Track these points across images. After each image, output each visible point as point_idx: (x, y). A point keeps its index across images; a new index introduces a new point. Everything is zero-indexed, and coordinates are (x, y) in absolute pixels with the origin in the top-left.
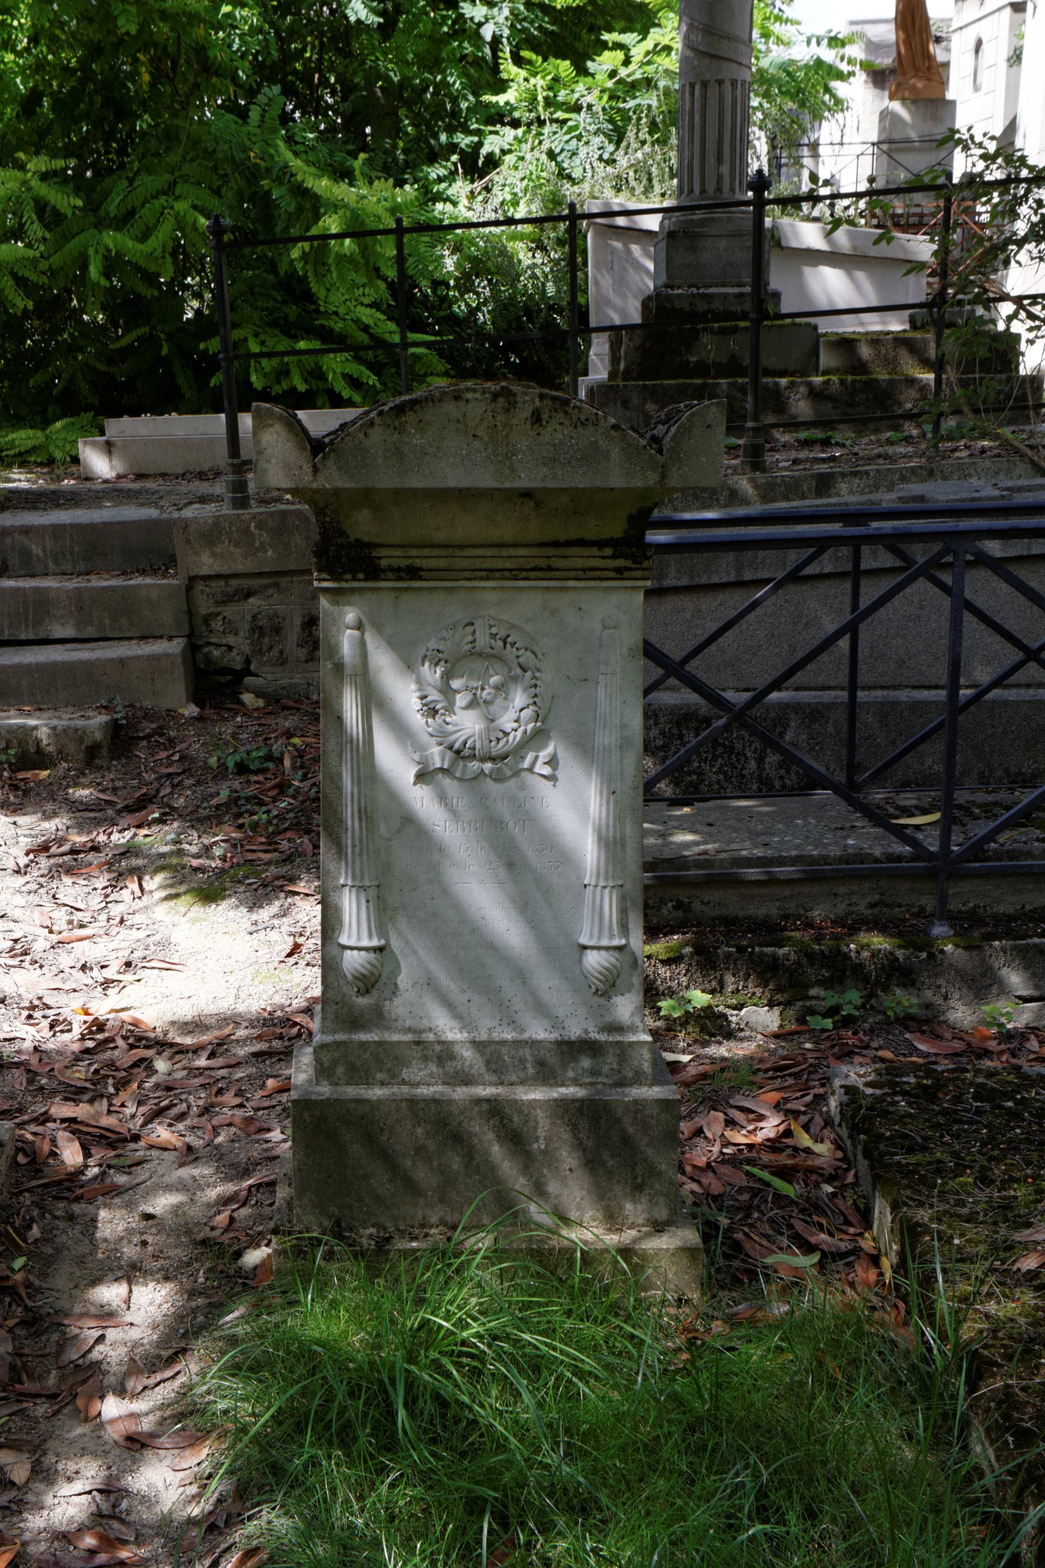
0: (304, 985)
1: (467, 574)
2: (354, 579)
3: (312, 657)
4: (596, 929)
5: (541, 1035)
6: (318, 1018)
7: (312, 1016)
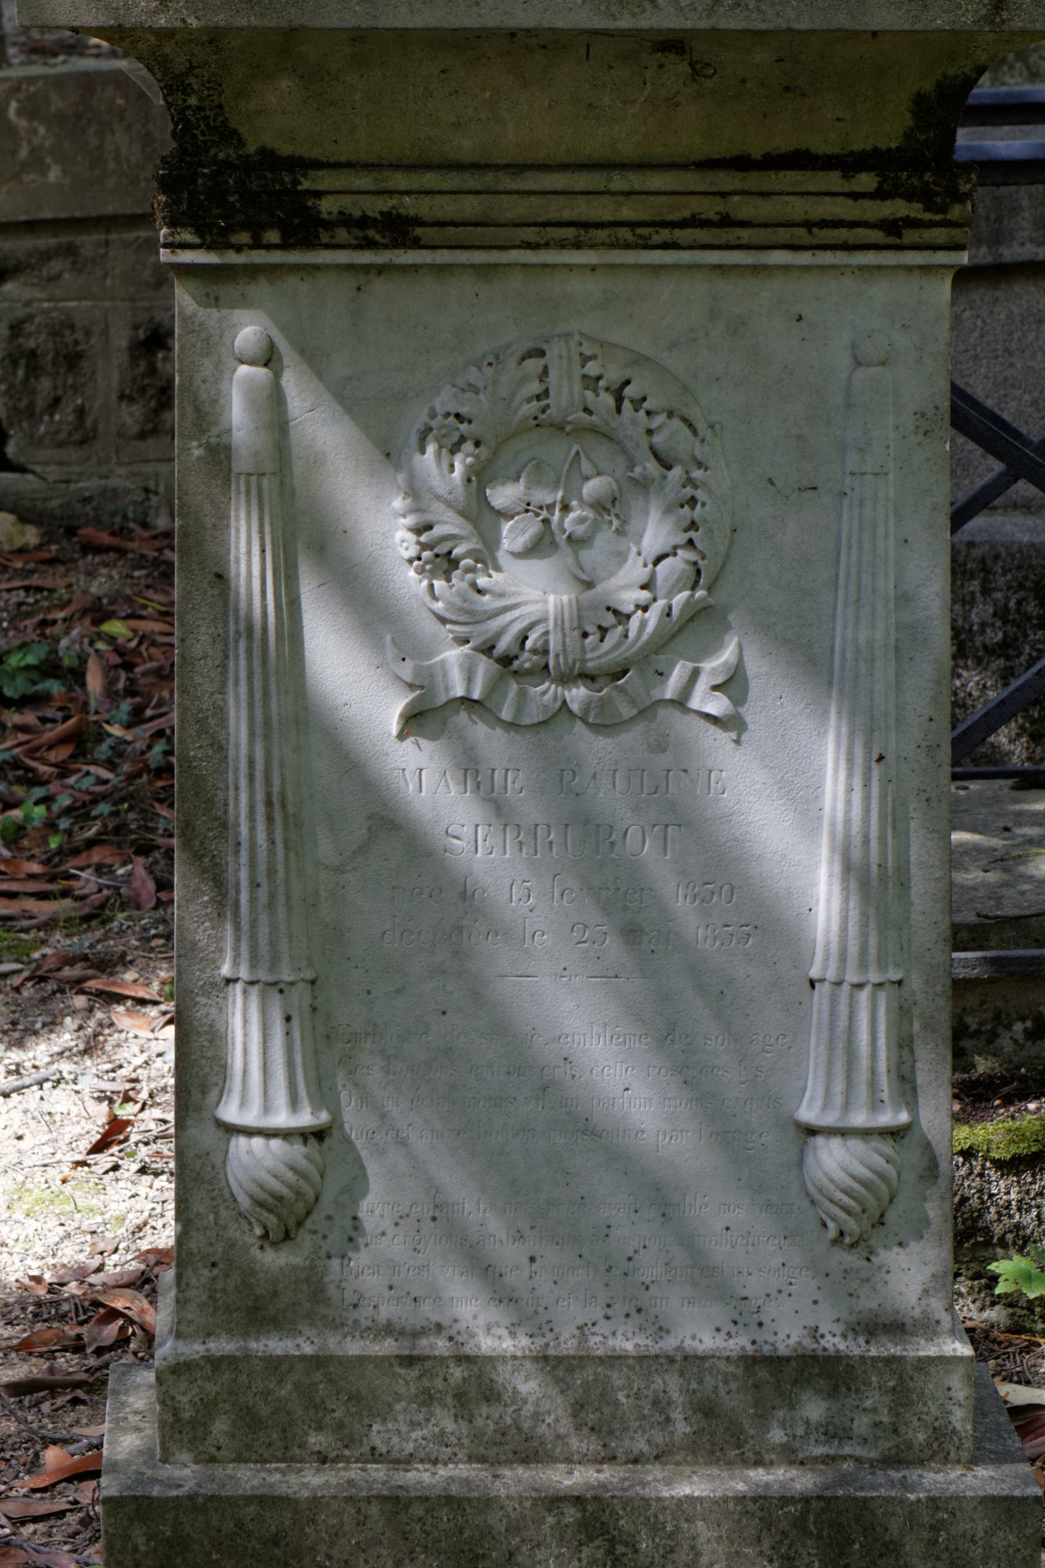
0: (134, 1219)
1: (530, 234)
2: (257, 244)
3: (155, 427)
4: (839, 1086)
5: (707, 1342)
6: (167, 1300)
7: (152, 1297)
